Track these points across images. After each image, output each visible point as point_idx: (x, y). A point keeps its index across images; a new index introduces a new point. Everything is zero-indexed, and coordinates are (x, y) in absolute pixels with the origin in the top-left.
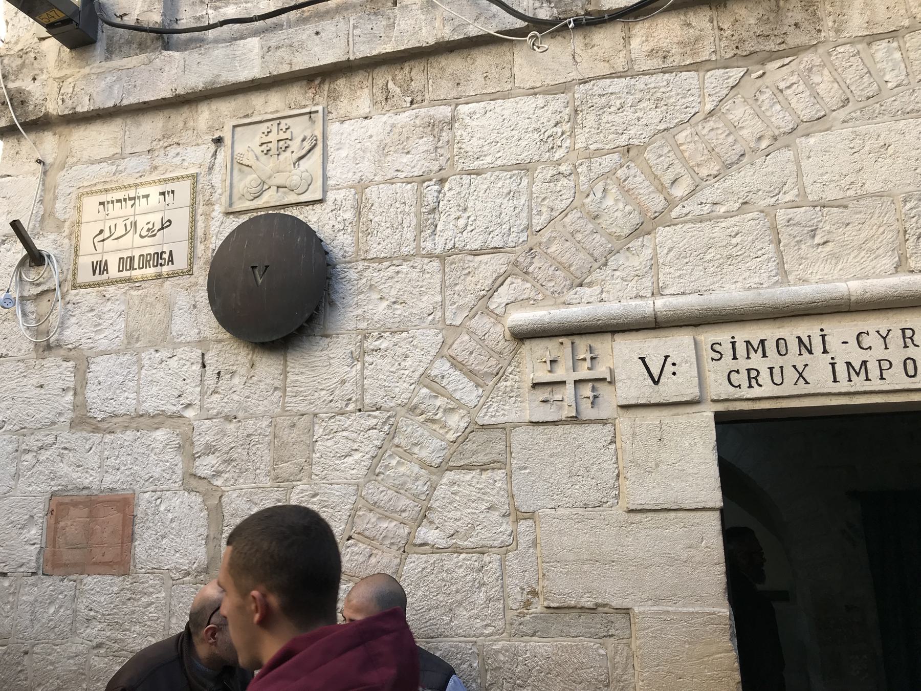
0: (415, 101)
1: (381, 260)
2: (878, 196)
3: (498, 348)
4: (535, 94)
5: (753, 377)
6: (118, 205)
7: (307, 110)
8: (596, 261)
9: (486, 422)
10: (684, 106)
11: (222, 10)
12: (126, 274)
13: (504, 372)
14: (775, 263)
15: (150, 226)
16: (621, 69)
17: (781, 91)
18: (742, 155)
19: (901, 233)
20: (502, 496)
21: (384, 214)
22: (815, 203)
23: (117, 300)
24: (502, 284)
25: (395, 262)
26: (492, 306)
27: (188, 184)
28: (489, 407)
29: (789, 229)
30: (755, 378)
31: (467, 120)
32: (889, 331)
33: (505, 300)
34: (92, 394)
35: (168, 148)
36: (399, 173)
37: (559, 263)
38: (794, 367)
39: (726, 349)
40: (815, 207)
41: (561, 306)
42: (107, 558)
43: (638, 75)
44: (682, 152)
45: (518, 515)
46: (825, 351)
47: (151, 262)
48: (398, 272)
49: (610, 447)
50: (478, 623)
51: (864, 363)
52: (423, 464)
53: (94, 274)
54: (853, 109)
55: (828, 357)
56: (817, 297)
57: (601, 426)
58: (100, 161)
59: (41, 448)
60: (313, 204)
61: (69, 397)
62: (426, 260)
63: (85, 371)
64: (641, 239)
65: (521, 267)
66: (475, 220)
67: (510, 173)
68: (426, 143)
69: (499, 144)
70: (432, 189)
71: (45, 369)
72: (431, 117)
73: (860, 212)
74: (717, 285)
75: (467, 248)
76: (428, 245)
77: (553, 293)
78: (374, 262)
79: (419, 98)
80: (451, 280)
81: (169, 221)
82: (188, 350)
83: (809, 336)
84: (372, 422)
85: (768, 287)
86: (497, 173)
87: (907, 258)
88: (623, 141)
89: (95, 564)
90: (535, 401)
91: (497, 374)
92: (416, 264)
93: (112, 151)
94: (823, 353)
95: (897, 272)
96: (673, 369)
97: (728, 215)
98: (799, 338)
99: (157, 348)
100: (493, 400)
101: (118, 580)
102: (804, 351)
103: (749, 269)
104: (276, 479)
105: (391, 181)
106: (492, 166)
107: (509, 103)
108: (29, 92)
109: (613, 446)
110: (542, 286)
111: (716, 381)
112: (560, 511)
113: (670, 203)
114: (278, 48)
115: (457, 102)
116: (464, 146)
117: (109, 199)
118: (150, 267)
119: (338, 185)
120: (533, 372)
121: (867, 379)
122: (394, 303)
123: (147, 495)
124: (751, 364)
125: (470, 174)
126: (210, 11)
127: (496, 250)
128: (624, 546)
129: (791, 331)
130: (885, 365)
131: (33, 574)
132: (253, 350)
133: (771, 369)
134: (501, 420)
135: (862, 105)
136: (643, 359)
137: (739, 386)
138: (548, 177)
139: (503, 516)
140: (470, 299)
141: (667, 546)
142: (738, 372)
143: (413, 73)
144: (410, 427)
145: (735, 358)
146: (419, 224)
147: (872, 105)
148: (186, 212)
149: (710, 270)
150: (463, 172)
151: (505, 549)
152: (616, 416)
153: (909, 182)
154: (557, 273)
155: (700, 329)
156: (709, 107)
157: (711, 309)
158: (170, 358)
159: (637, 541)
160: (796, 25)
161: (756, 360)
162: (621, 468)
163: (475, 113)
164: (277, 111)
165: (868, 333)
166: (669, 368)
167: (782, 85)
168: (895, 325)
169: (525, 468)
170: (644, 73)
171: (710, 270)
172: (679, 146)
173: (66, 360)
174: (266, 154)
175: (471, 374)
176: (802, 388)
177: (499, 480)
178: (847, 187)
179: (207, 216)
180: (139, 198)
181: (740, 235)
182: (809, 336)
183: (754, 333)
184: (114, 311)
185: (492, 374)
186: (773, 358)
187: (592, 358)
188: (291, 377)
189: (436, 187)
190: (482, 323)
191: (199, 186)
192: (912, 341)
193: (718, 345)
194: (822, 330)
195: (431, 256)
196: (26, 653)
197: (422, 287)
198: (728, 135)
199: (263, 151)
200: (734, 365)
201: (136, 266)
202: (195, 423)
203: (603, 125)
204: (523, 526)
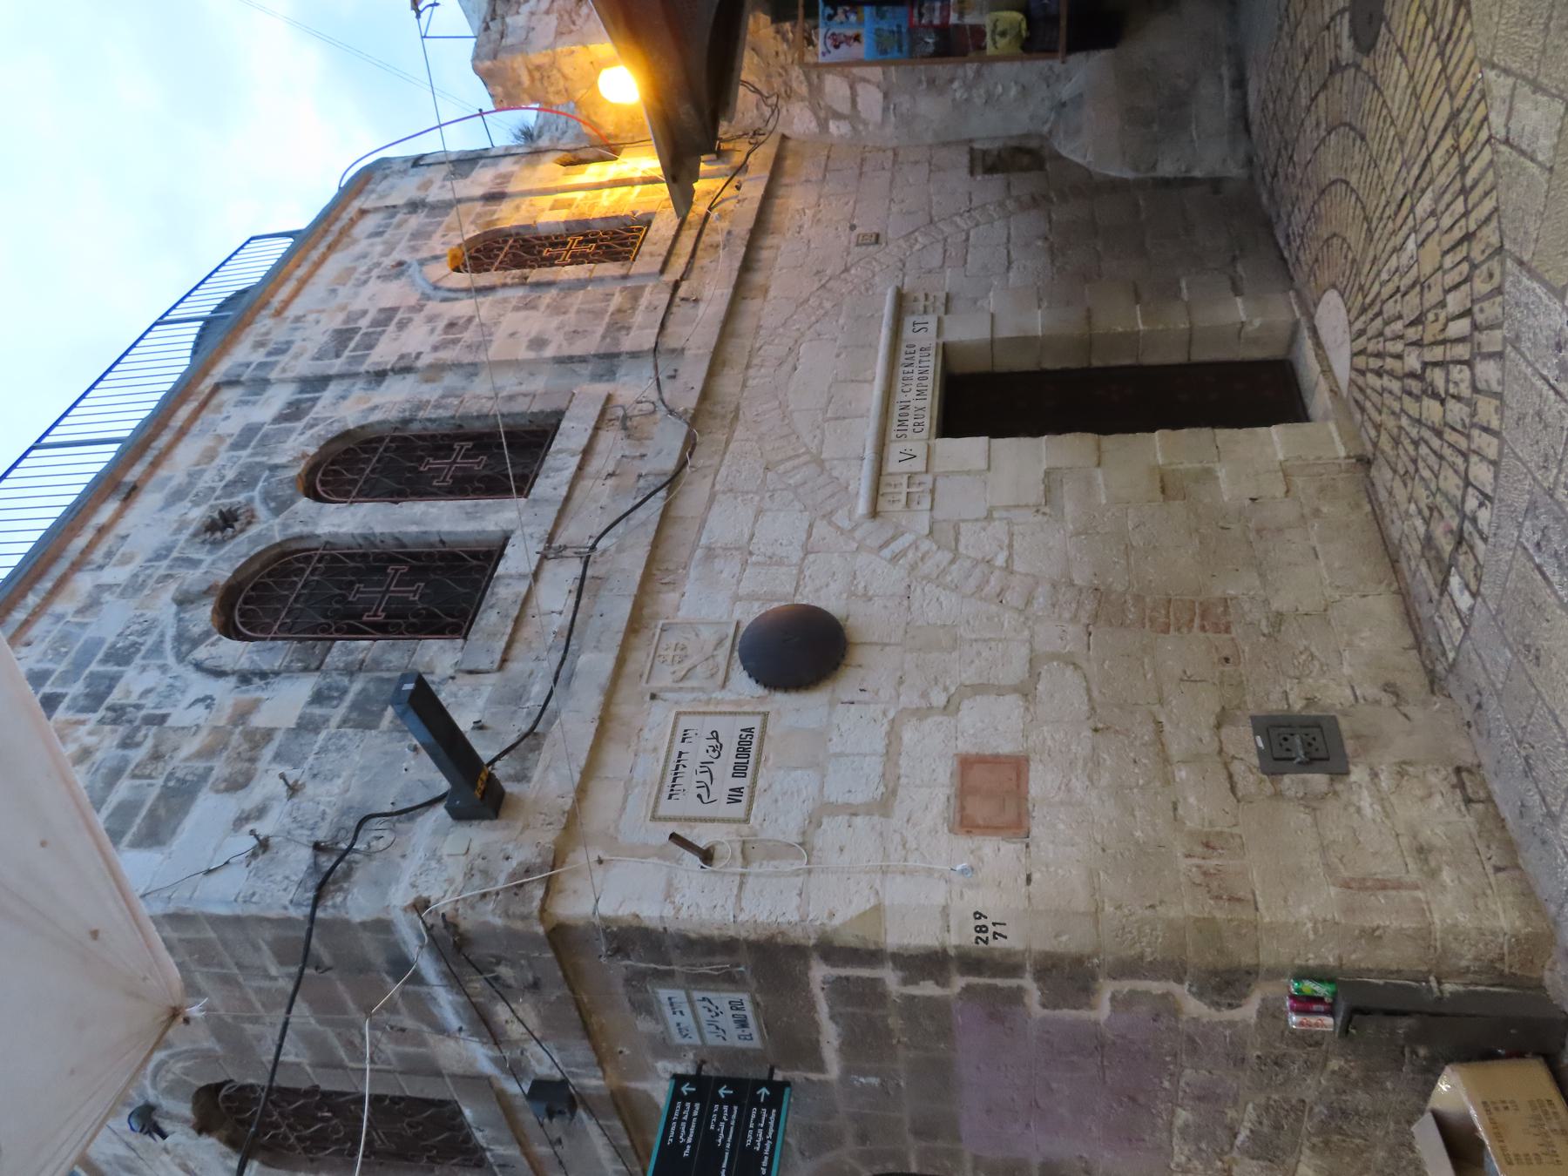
7: (658, 631)
11: (533, 695)
12: (749, 772)
34: (859, 798)
39: (900, 433)
42: (1014, 776)
45: (989, 517)
50: (1057, 536)
52: (953, 562)
59: (904, 846)
61: (858, 821)
68: (718, 564)
70: (754, 558)
76: (795, 558)
84: (919, 590)
89: (1018, 786)
97: (823, 433)
101: (1033, 766)
104: (954, 649)
105: (739, 582)
108: (520, 864)
114: (599, 641)
123: (960, 743)
126: (528, 704)
127: (811, 526)
129: (896, 411)
131: (1027, 846)
132: (846, 666)
144: (927, 567)
148: (708, 718)
151: (1010, 523)
161: (911, 422)
164: (648, 655)
170: (722, 461)
173: (820, 825)
175: (893, 538)
179: (718, 703)
188: (875, 639)
190: (858, 534)
195: (803, 559)
196: (1104, 850)
202: (901, 707)
204: (996, 515)
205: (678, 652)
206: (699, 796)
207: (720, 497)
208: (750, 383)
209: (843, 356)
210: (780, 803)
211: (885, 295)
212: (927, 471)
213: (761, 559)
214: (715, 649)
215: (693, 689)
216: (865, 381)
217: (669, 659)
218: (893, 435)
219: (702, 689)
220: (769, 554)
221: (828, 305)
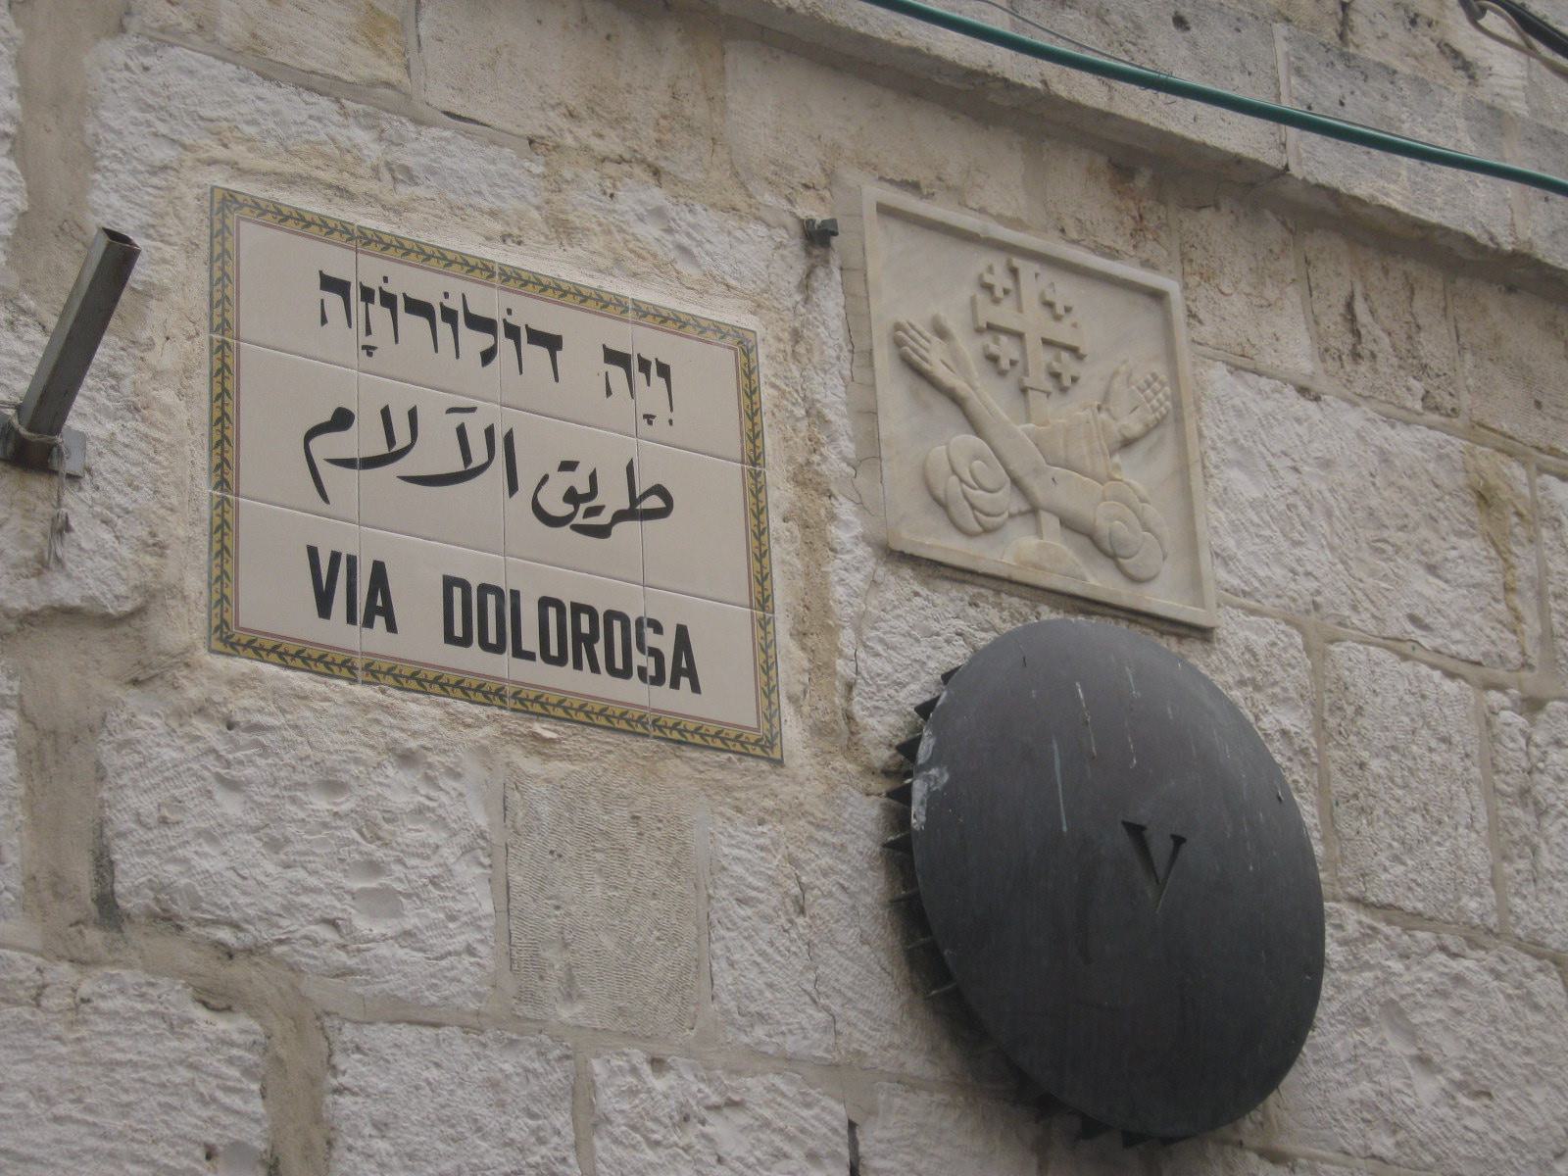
0: (1430, 402)
1: (1413, 920)
6: (414, 326)
12: (473, 660)
15: (580, 482)
21: (1395, 757)
23: (456, 775)
25: (1449, 940)
27: (723, 360)
35: (610, 169)
36: (1417, 634)
47: (599, 648)
48: (1458, 979)
53: (324, 608)
58: (309, 83)
60: (1180, 637)
62: (1530, 964)
63: (314, 1082)
71: (103, 1026)
76: (1530, 911)
78: (1389, 922)
79: (1448, 403)
81: (659, 490)
82: (790, 1090)
92: (1503, 969)
93: (363, 64)
99: (659, 1050)
105: (1397, 646)
117: (374, 284)
118: (595, 669)
119: (1244, 593)
122: (1461, 1086)
143: (1419, 303)
146: (1497, 827)
158: (716, 1108)
174: (1002, 373)
180: (512, 332)
184: (441, 822)
189: (1520, 721)
191: (766, 394)
195: (1535, 948)
197: (1528, 1051)
199: (993, 359)
201: (530, 641)
205: (1044, 357)
206: (342, 420)
210: (321, 804)
213: (1512, 750)
214: (1070, 525)
215: (868, 414)
217: (1004, 315)
219: (870, 455)
220: (1543, 783)
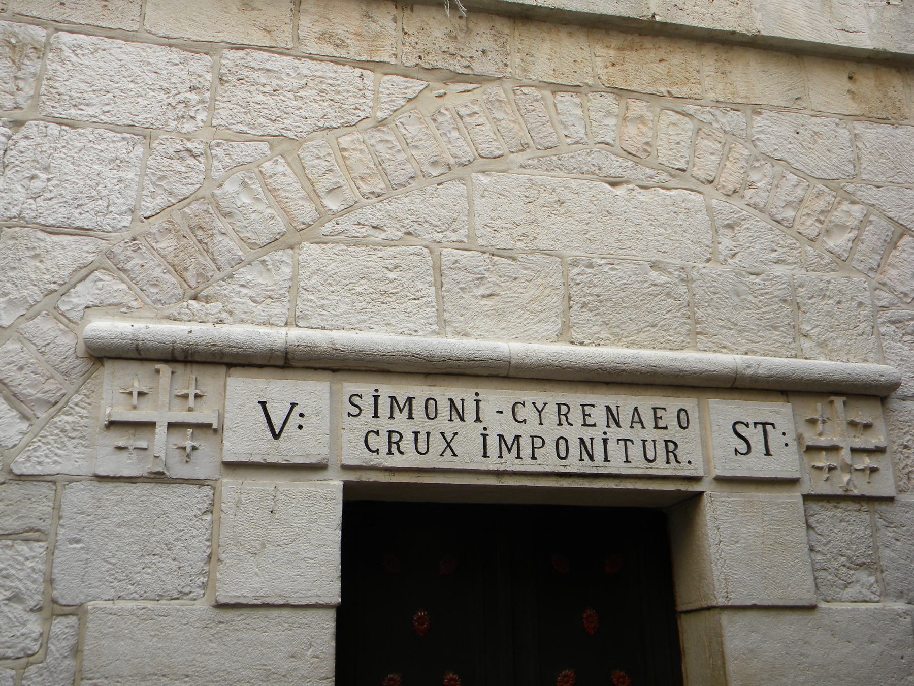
2: (547, 254)
3: (65, 366)
4: (170, 47)
5: (394, 442)
8: (219, 269)
9: (25, 471)
10: (354, 107)
13: (67, 402)
14: (434, 310)
16: (283, 45)
17: (461, 117)
18: (412, 178)
19: (566, 298)
20: (34, 581)
22: (484, 249)
24: (84, 279)
26: (63, 308)
28: (35, 450)
29: (453, 272)
30: (397, 443)
31: (67, 53)
32: (545, 404)
33: (83, 302)
37: (169, 263)
38: (443, 434)
39: (367, 403)
40: (484, 253)
41: (164, 321)
43: (303, 57)
44: (344, 158)
46: (478, 420)
49: (204, 517)
51: (517, 437)
54: (531, 156)
55: (480, 426)
56: (477, 354)
57: (193, 489)
64: (280, 253)
65: (116, 261)
66: (56, 186)
67: (119, 135)
69: (110, 96)
72: (15, 35)
73: (529, 268)
74: (365, 324)
75: (38, 221)
77: (155, 302)
80: (7, 260)
83: (462, 400)
85: (425, 336)
86: (101, 131)
87: (570, 328)
88: (272, 129)
90: (107, 446)
91: (56, 403)
94: (475, 421)
95: (558, 341)
96: (300, 421)
97: (387, 243)
98: (451, 400)
100: (44, 440)
102: (455, 417)
103: (404, 311)
106: (94, 120)
107: (130, 47)
109: (208, 517)
110: (142, 290)
111: (350, 442)
112: (120, 604)
113: (323, 215)
115: (57, 26)
116: (57, 85)
120: (111, 406)
121: (519, 457)
124: (393, 425)
125: (60, 124)
127: (83, 231)
128: (205, 654)
129: (443, 393)
130: (538, 443)
133: (416, 434)
134: (49, 468)
135: (540, 153)
136: (263, 404)
137: (377, 451)
138: (171, 151)
139: (31, 610)
140: (33, 293)
141: (263, 655)
142: (377, 433)
145: (376, 416)
147: (550, 156)
149: (358, 305)
150: (49, 119)
152: (217, 476)
153: (578, 245)
154: (166, 276)
155: (338, 376)
156: (380, 115)
157: (356, 352)
159: (224, 647)
160: (484, 52)
161: (401, 422)
162: (215, 546)
163: (80, 47)
165: (524, 405)
166: (295, 420)
167: (463, 111)
168: (551, 398)
169: (78, 541)
170: (311, 57)
171: (358, 305)
172: (343, 150)
176: (448, 462)
177: (34, 557)
178: (518, 238)
181: (398, 269)
182: (462, 400)
183: (403, 390)
185: (49, 402)
186: (420, 422)
187: (197, 396)
190: (45, 327)
192: (567, 418)
193: (357, 398)
194: (477, 394)
198: (399, 151)
200: (374, 425)
203: (252, 104)
207: (200, 64)
208: (566, 101)
209: (654, 275)
211: (883, 360)
212: (232, 466)
216: (567, 326)
218: (351, 386)
221: (838, 242)
